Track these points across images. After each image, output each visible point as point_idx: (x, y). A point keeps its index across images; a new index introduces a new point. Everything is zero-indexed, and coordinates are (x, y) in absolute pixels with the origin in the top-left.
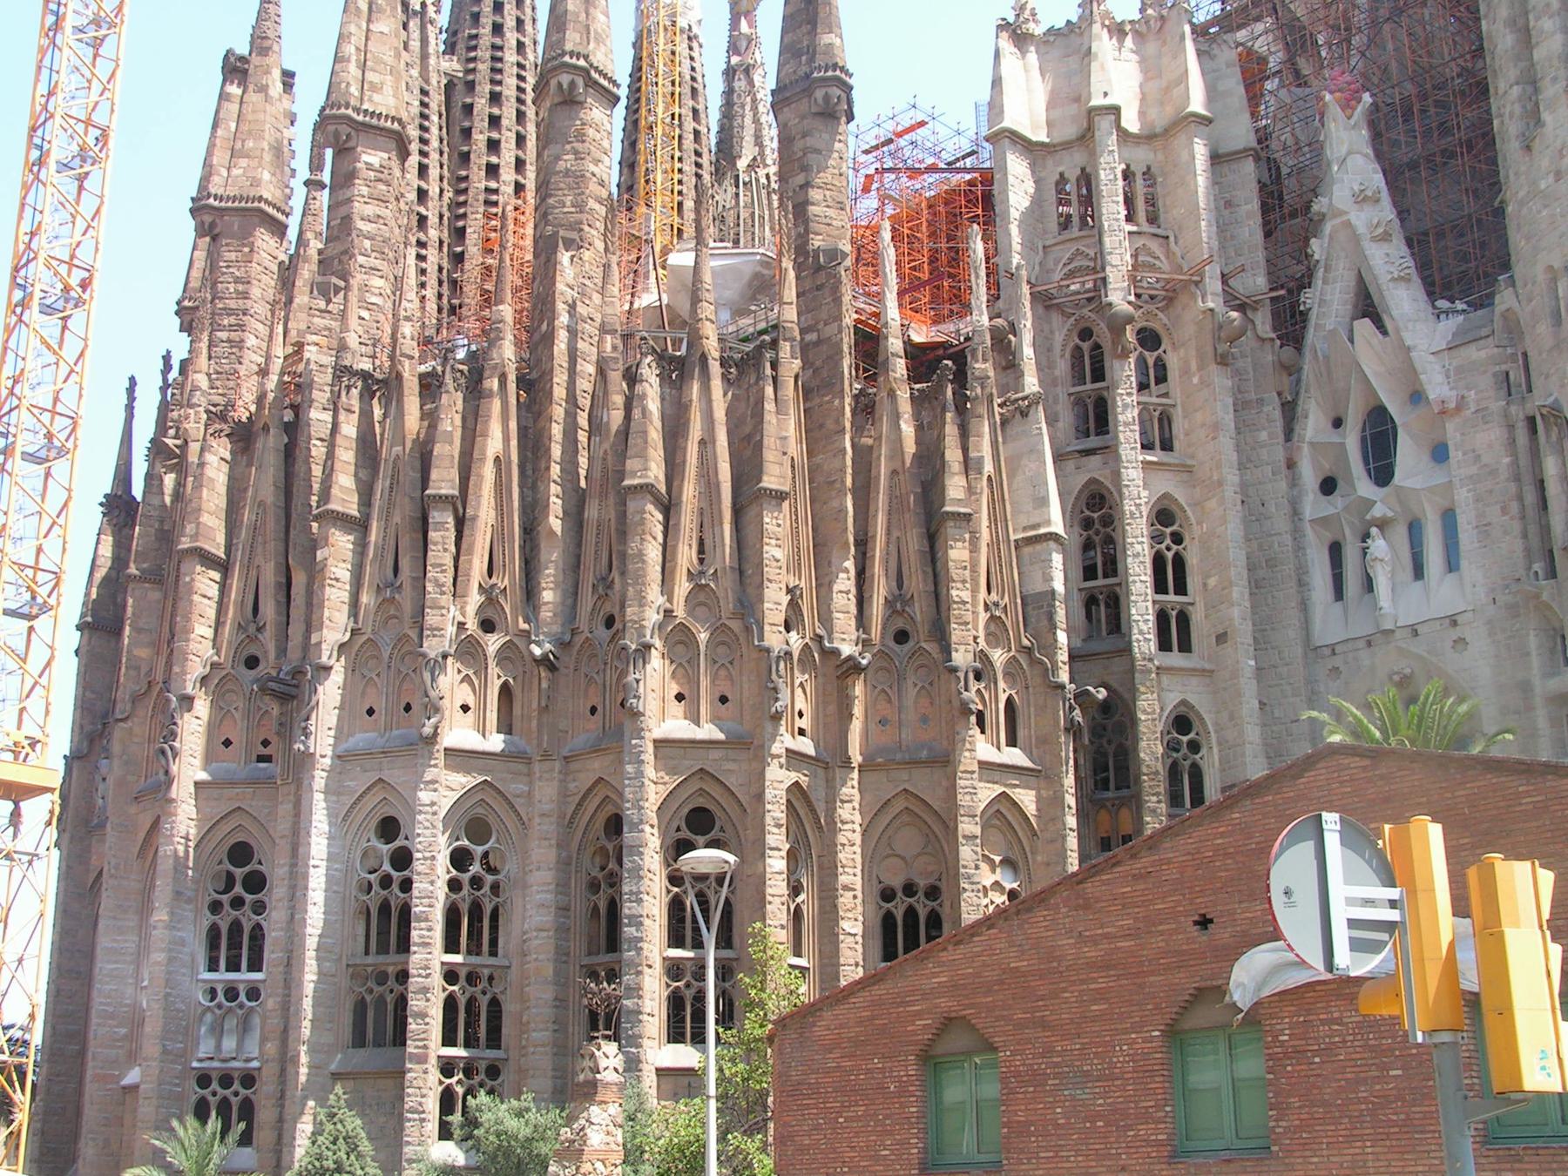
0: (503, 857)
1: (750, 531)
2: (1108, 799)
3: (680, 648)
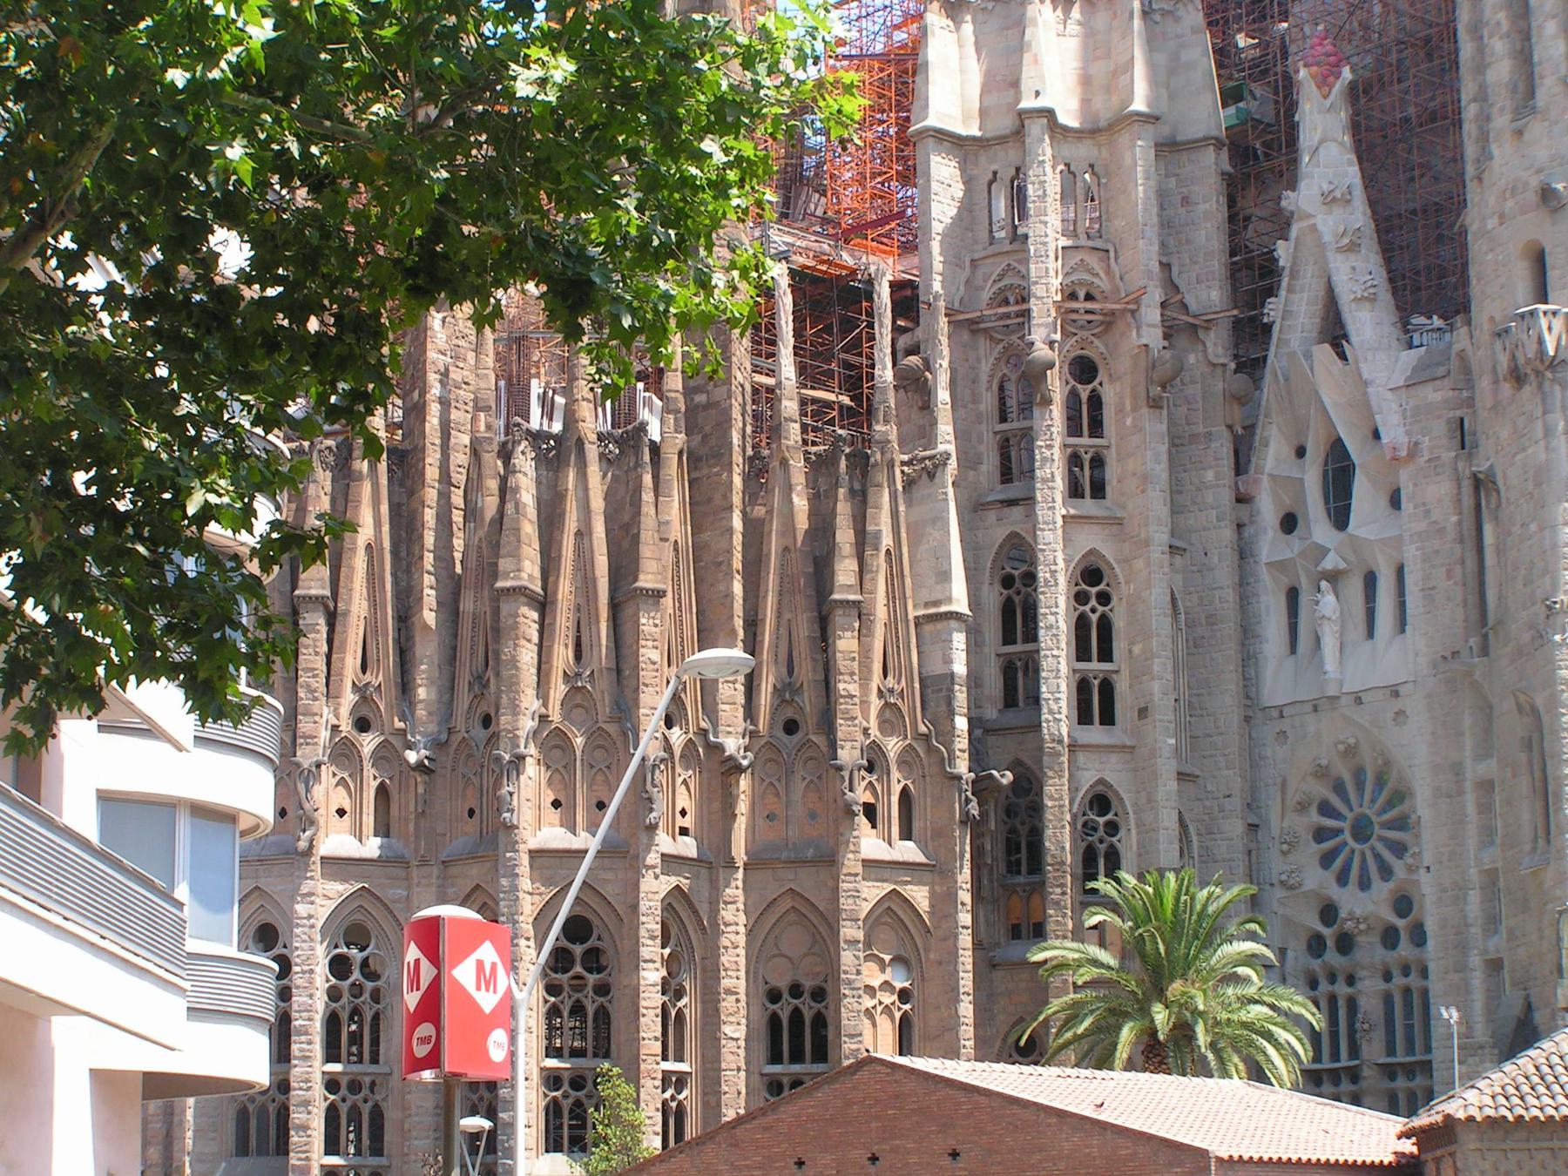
0: (383, 964)
1: (627, 628)
2: (1019, 885)
3: (557, 753)
